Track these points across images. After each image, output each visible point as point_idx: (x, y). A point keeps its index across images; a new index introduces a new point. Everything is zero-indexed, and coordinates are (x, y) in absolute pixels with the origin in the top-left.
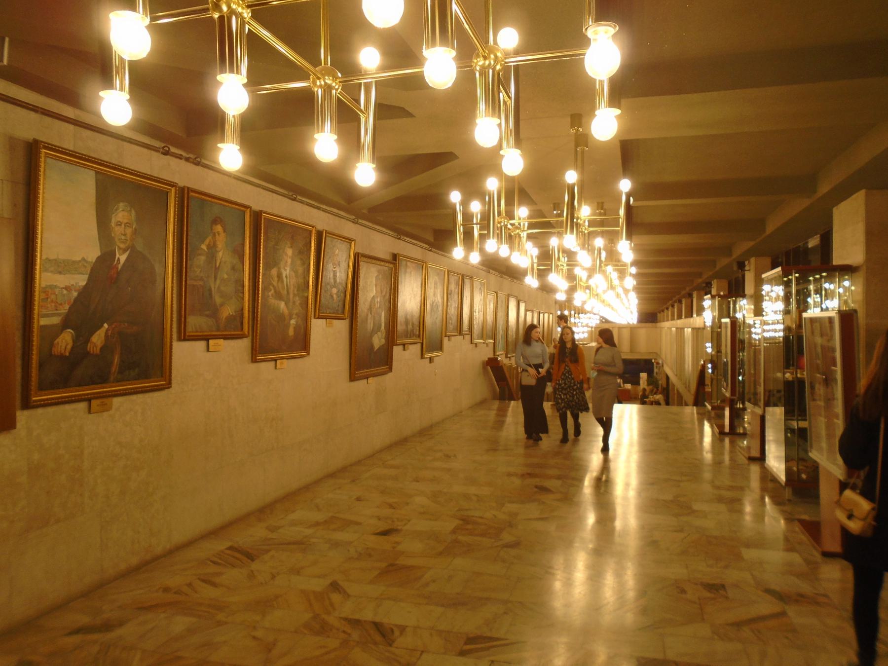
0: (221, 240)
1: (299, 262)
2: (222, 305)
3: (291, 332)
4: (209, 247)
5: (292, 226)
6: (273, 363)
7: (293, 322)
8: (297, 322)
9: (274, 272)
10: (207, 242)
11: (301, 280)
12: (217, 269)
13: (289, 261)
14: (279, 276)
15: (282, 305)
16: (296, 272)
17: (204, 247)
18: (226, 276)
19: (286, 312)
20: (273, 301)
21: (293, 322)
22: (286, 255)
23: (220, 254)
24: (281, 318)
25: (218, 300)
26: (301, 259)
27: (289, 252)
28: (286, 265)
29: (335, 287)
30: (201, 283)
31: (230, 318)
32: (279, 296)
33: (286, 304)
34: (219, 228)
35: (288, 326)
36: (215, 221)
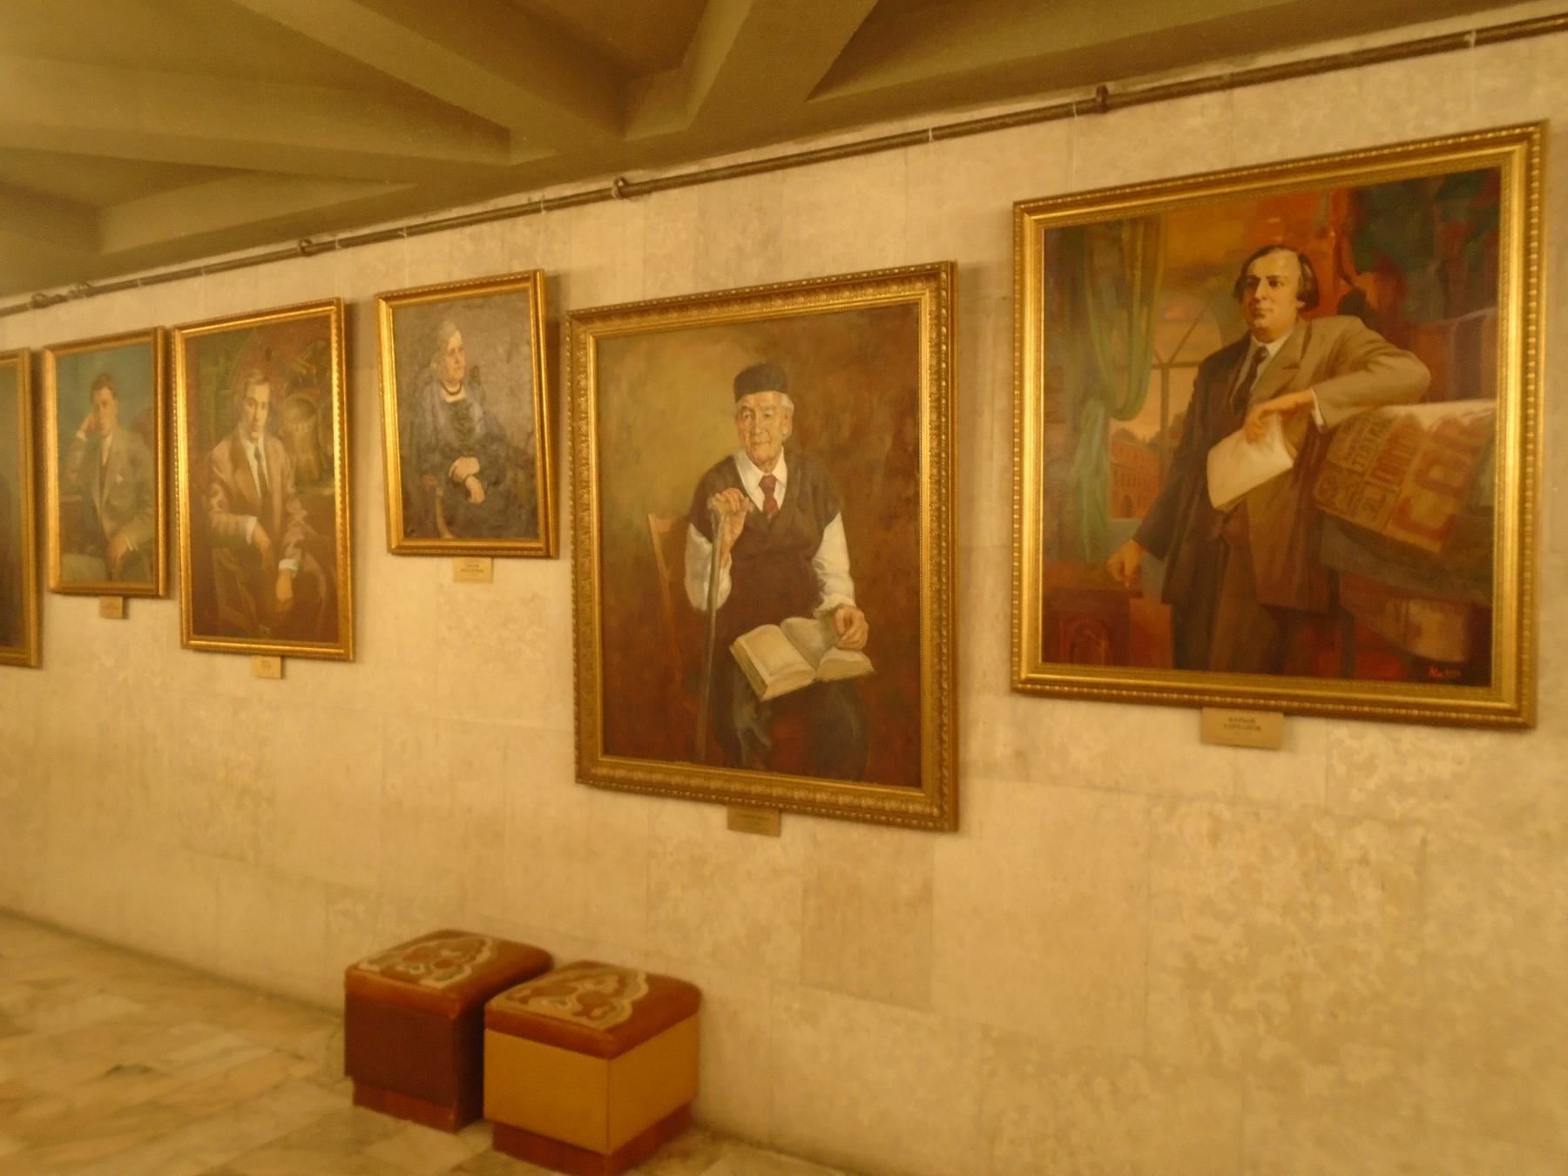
0: (109, 417)
1: (293, 412)
2: (115, 533)
3: (284, 590)
4: (89, 433)
5: (262, 328)
6: (276, 662)
7: (287, 565)
8: (301, 568)
9: (222, 451)
10: (85, 425)
11: (307, 457)
12: (104, 470)
13: (263, 415)
14: (238, 458)
15: (251, 525)
16: (286, 440)
17: (81, 435)
18: (119, 479)
19: (263, 540)
20: (222, 519)
21: (287, 565)
22: (253, 402)
23: (109, 440)
24: (247, 553)
25: (108, 526)
26: (301, 402)
27: (261, 393)
28: (253, 426)
29: (468, 451)
30: (79, 498)
31: (132, 559)
32: (239, 504)
33: (260, 521)
34: (105, 393)
35: (275, 573)
36: (97, 386)
